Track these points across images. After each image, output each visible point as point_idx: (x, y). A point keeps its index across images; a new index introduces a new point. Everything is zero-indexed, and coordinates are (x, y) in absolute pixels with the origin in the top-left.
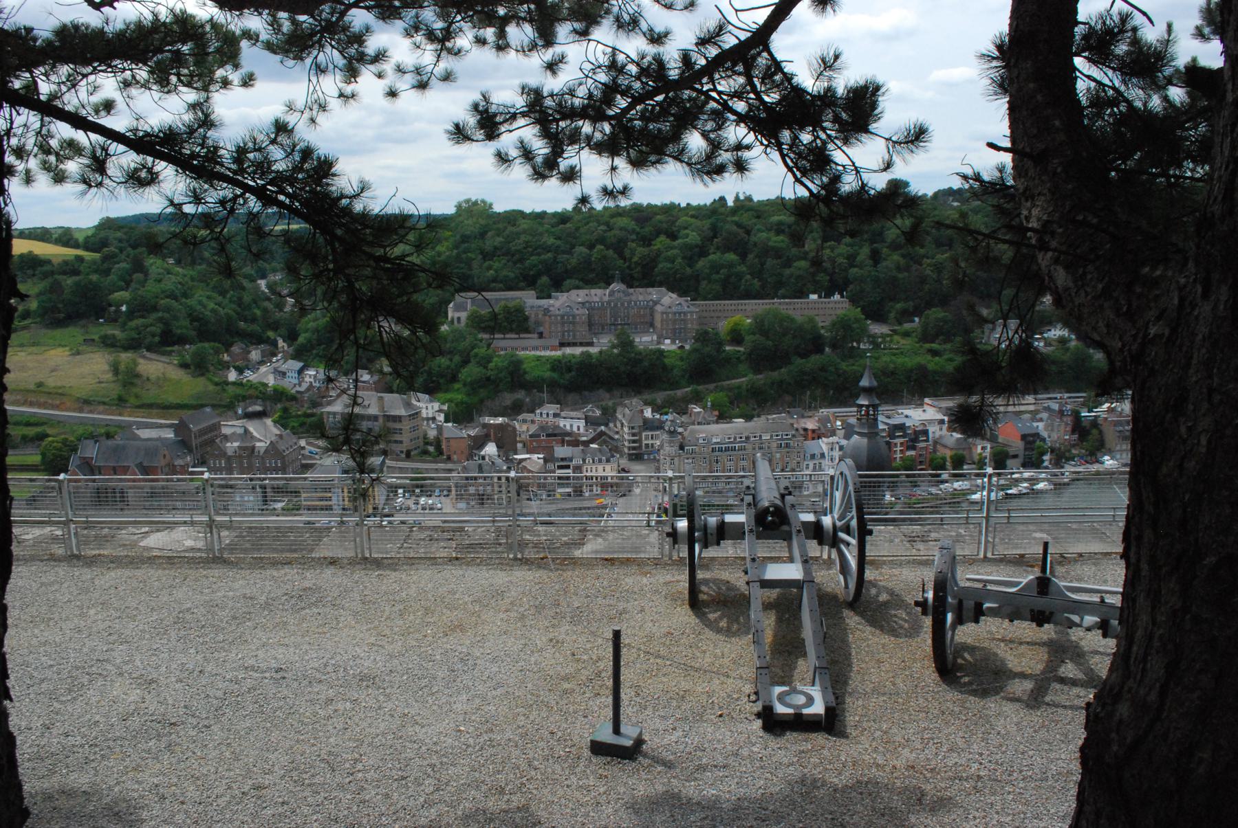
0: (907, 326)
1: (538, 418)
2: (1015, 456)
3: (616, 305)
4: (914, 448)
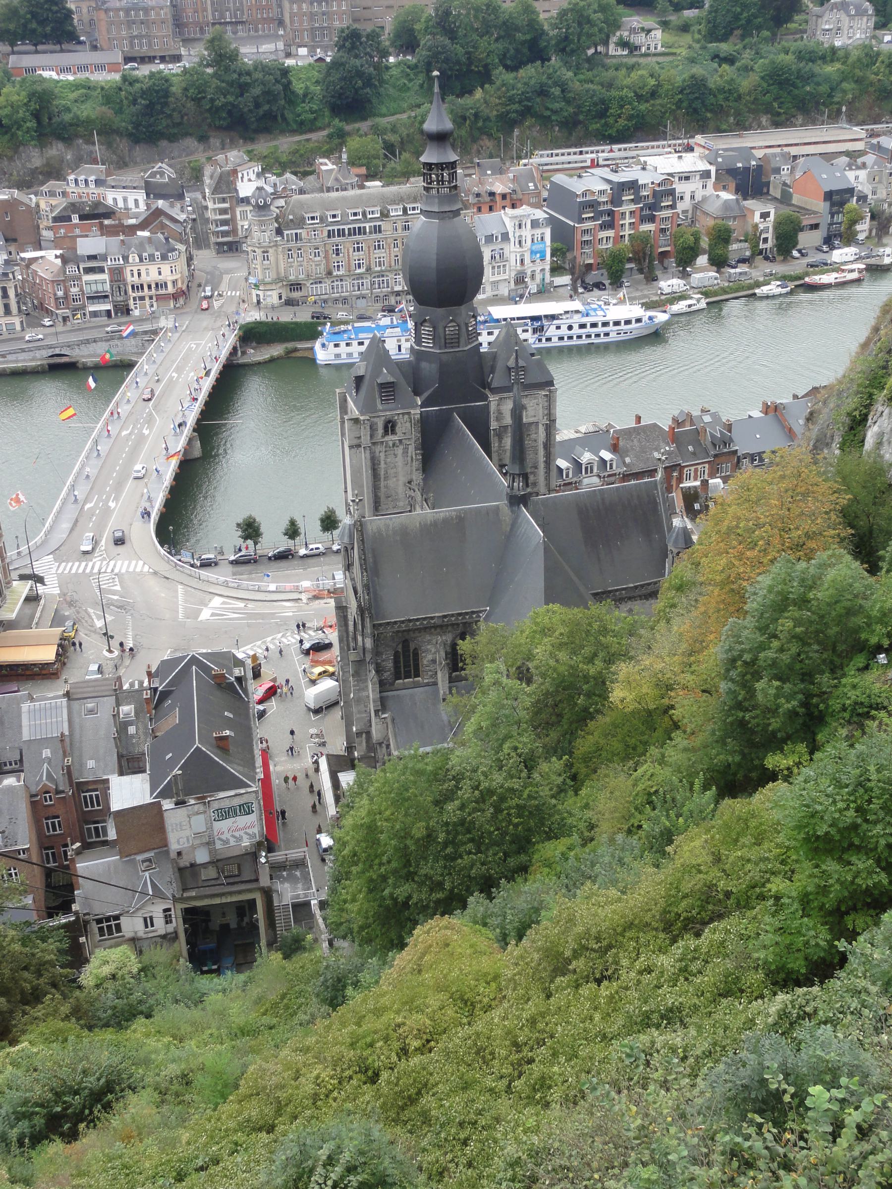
0: (689, 14)
1: (71, 188)
2: (815, 227)
4: (652, 219)
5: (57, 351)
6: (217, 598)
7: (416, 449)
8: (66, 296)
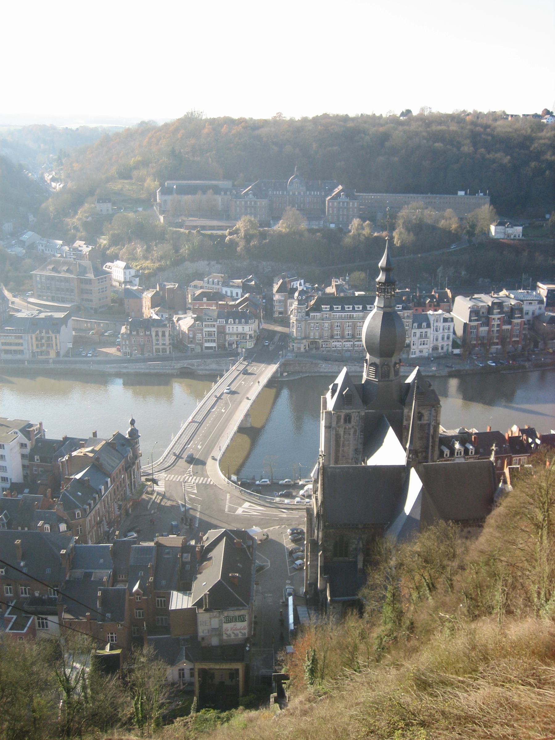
3: (294, 194)
4: (510, 323)
6: (247, 503)
7: (361, 432)
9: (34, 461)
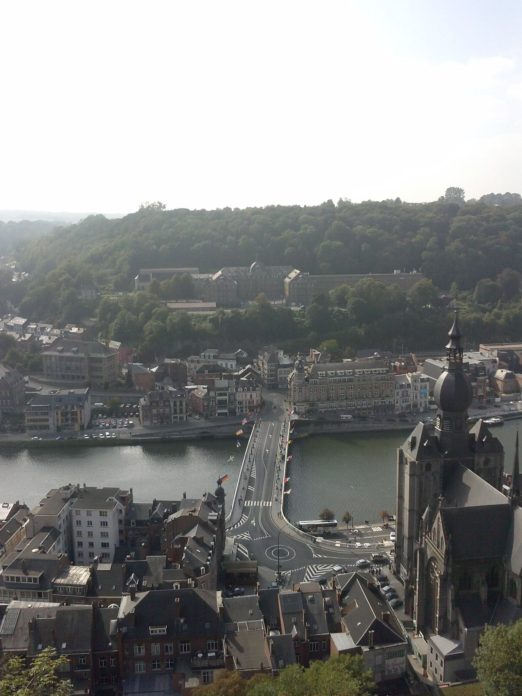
5: (205, 430)
8: (208, 406)
9: (130, 525)
